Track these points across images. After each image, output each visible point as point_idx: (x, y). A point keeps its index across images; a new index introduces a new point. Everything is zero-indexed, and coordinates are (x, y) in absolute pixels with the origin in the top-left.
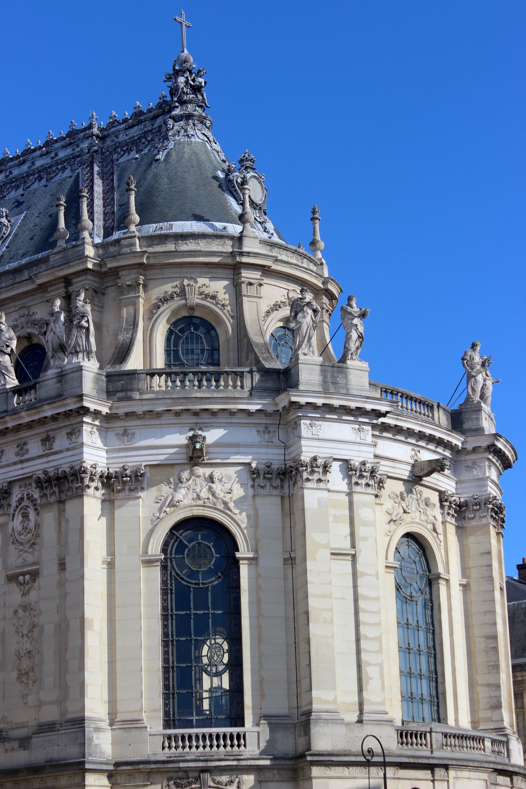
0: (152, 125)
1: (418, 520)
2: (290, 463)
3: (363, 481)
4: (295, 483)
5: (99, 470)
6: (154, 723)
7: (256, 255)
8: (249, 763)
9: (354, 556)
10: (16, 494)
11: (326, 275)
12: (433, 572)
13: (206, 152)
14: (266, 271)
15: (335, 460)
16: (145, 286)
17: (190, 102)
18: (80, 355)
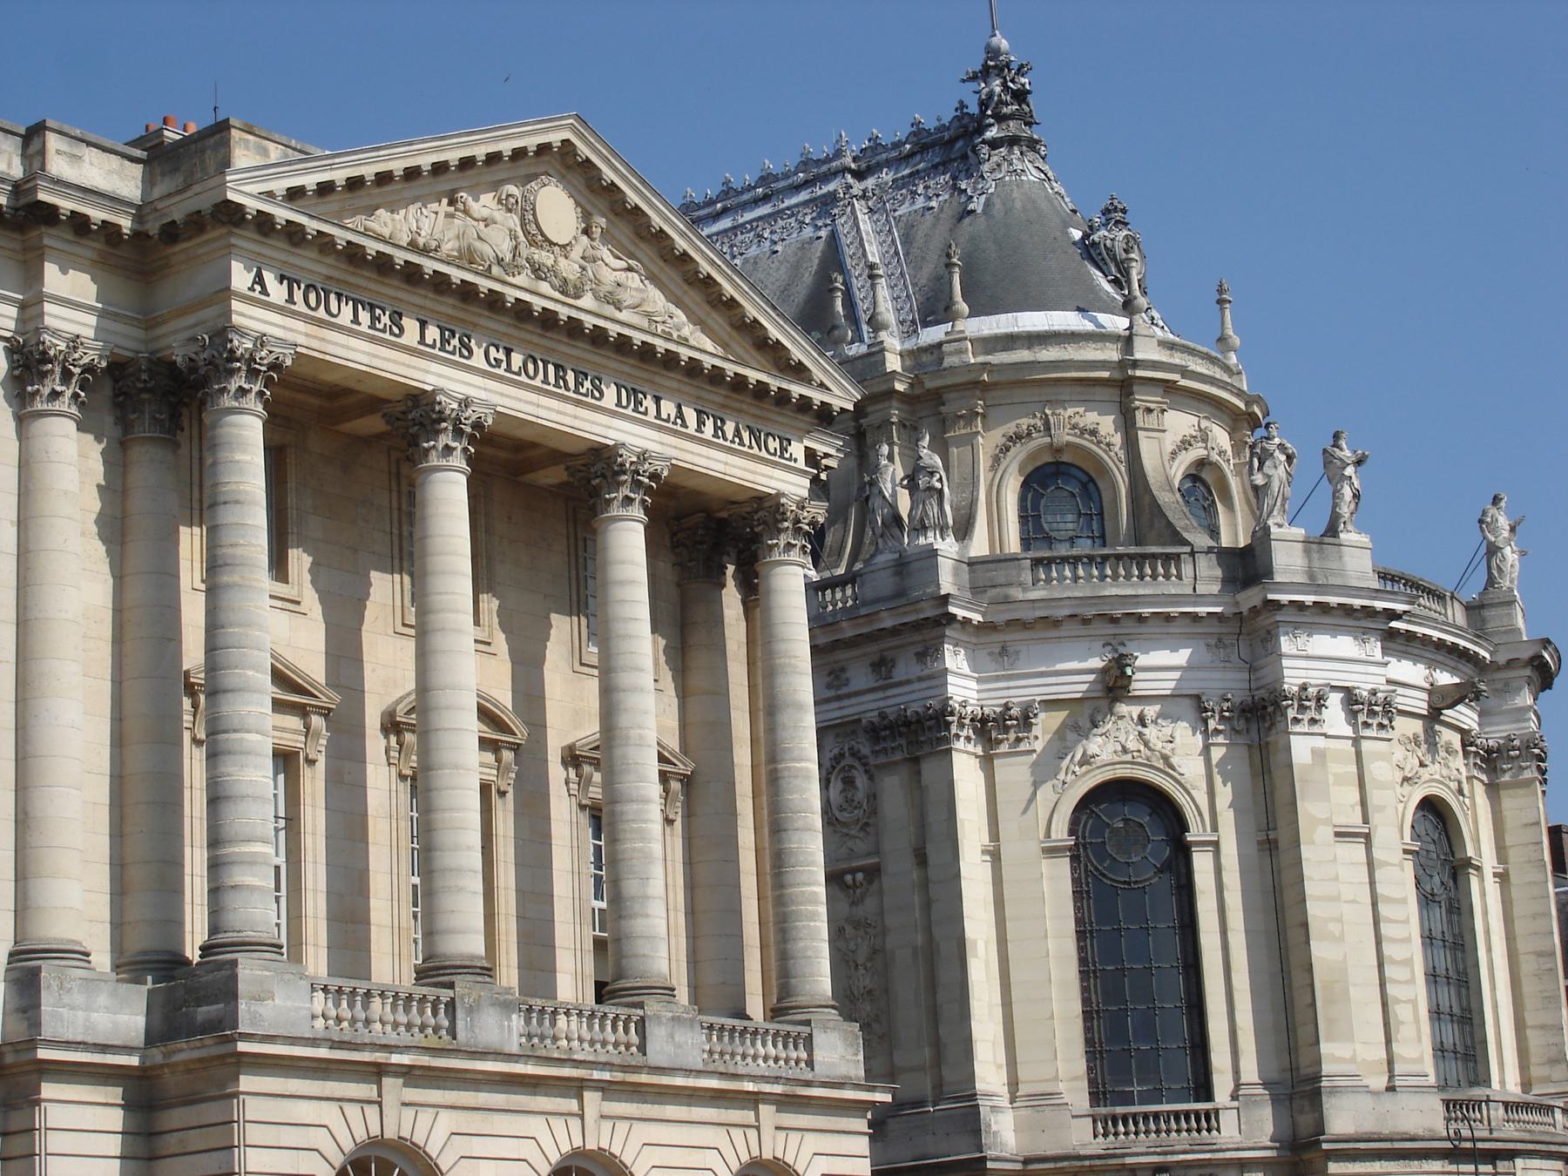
1: (1437, 777)
2: (1262, 693)
3: (1375, 722)
4: (1273, 724)
6: (1077, 1095)
7: (1155, 365)
8: (1228, 1155)
9: (1367, 836)
12: (1458, 856)
13: (1047, 196)
17: (1011, 117)
18: (930, 534)
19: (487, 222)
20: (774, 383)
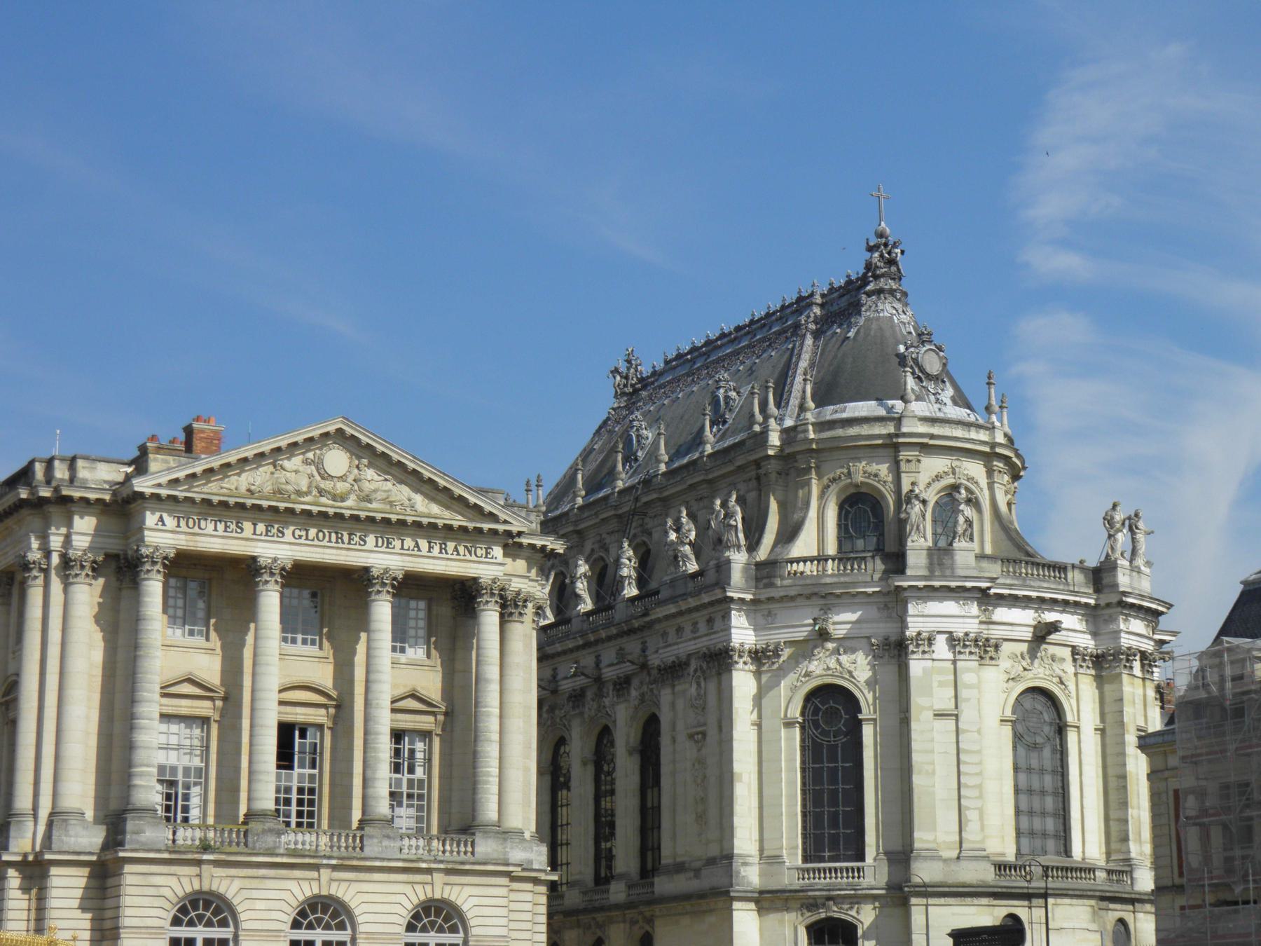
0: (845, 302)
3: (967, 650)
5: (747, 647)
6: (793, 856)
9: (957, 716)
10: (694, 664)
11: (1000, 438)
14: (924, 448)
15: (939, 632)
16: (817, 467)
17: (883, 275)
19: (296, 472)
20: (471, 525)
